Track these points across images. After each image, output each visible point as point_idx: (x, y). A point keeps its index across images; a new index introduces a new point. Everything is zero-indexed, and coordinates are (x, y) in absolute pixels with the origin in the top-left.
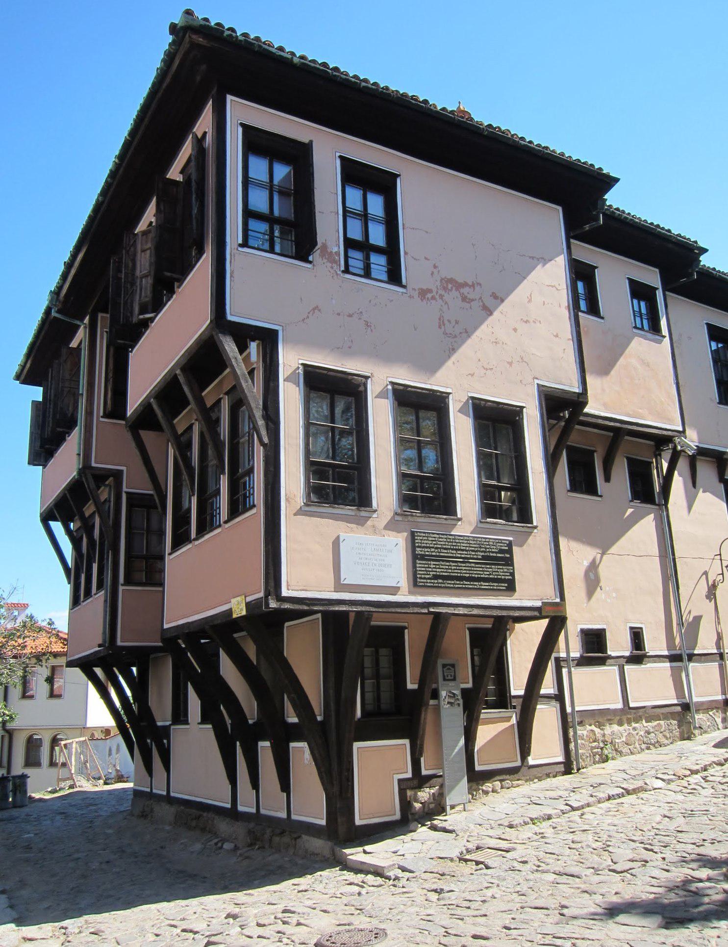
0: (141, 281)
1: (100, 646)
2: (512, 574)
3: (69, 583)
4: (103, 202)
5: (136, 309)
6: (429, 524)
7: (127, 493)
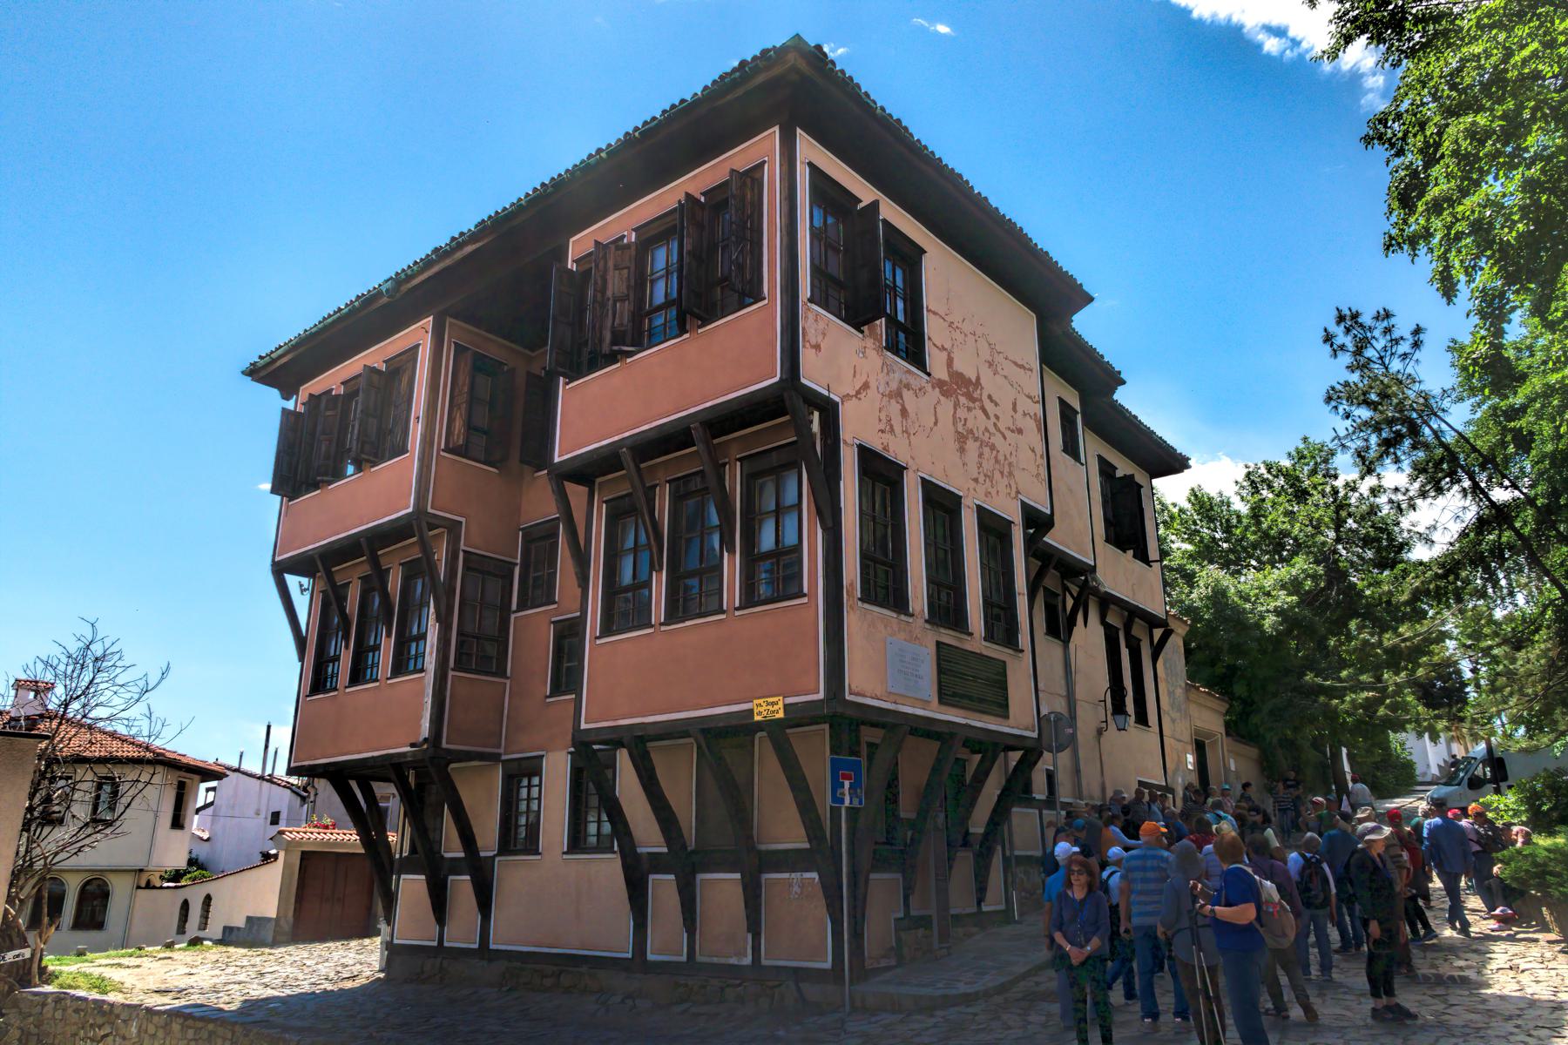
3: (301, 659)
5: (608, 336)
6: (948, 637)
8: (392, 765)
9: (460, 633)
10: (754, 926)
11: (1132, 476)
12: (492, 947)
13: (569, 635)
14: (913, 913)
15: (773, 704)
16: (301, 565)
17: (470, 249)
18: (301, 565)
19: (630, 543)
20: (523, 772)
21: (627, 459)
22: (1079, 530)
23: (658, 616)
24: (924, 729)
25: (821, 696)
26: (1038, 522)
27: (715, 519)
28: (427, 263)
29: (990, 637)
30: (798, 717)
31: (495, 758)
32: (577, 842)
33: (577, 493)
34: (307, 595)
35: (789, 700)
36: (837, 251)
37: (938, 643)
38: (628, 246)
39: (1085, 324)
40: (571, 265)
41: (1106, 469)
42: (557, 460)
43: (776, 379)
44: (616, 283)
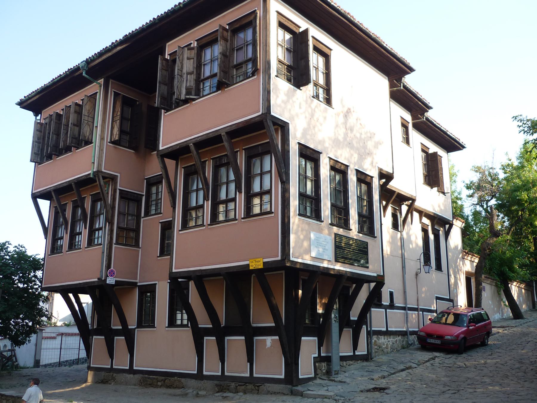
0: (187, 76)
3: (46, 238)
4: (157, 23)
5: (184, 91)
6: (341, 231)
7: (119, 189)
9: (118, 228)
10: (250, 360)
11: (437, 152)
12: (135, 368)
13: (167, 227)
14: (322, 355)
15: (258, 262)
17: (119, 48)
18: (45, 195)
19: (195, 187)
26: (386, 177)
27: (232, 177)
28: (100, 54)
30: (269, 267)
31: (135, 284)
32: (172, 323)
33: (170, 163)
35: (266, 260)
38: (193, 49)
39: (410, 81)
41: (424, 150)
42: (161, 148)
43: (260, 113)
44: (188, 66)
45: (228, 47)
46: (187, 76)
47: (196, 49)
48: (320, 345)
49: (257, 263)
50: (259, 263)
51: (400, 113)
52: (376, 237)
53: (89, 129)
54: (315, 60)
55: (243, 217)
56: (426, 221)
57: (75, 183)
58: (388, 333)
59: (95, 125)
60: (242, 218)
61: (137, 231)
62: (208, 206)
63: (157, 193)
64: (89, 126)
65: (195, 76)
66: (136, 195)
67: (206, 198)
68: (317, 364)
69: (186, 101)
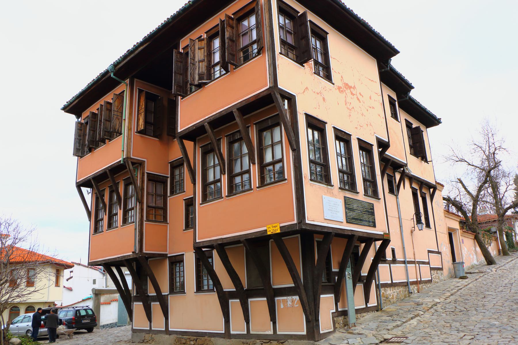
0: (199, 64)
1: (133, 252)
2: (375, 219)
3: (90, 221)
5: (197, 78)
6: (349, 195)
7: (147, 173)
8: (126, 260)
9: (148, 206)
10: (273, 319)
13: (190, 203)
14: (339, 310)
15: (275, 227)
16: (86, 183)
18: (86, 183)
19: (212, 164)
20: (177, 261)
21: (207, 127)
22: (400, 150)
23: (225, 192)
24: (340, 234)
25: (295, 222)
26: (384, 145)
27: (245, 150)
28: (125, 57)
29: (366, 194)
31: (165, 256)
32: (199, 288)
33: (189, 145)
34: (90, 194)
36: (290, 33)
37: (345, 197)
38: (203, 40)
39: (395, 62)
40: (181, 51)
41: (409, 125)
42: (179, 131)
43: (268, 87)
44: (200, 55)
45: (234, 33)
46: (199, 64)
47: (205, 40)
48: (337, 301)
49: (274, 228)
50: (276, 228)
51: (388, 92)
52: (379, 199)
53: (118, 123)
54: (314, 42)
55: (257, 186)
56: (415, 186)
57: (109, 170)
58: (393, 285)
59: (124, 118)
60: (258, 188)
61: (164, 209)
62: (225, 179)
63: (180, 174)
64: (119, 119)
65: (206, 63)
66: (161, 177)
67: (222, 172)
68: (335, 319)
69: (200, 86)
